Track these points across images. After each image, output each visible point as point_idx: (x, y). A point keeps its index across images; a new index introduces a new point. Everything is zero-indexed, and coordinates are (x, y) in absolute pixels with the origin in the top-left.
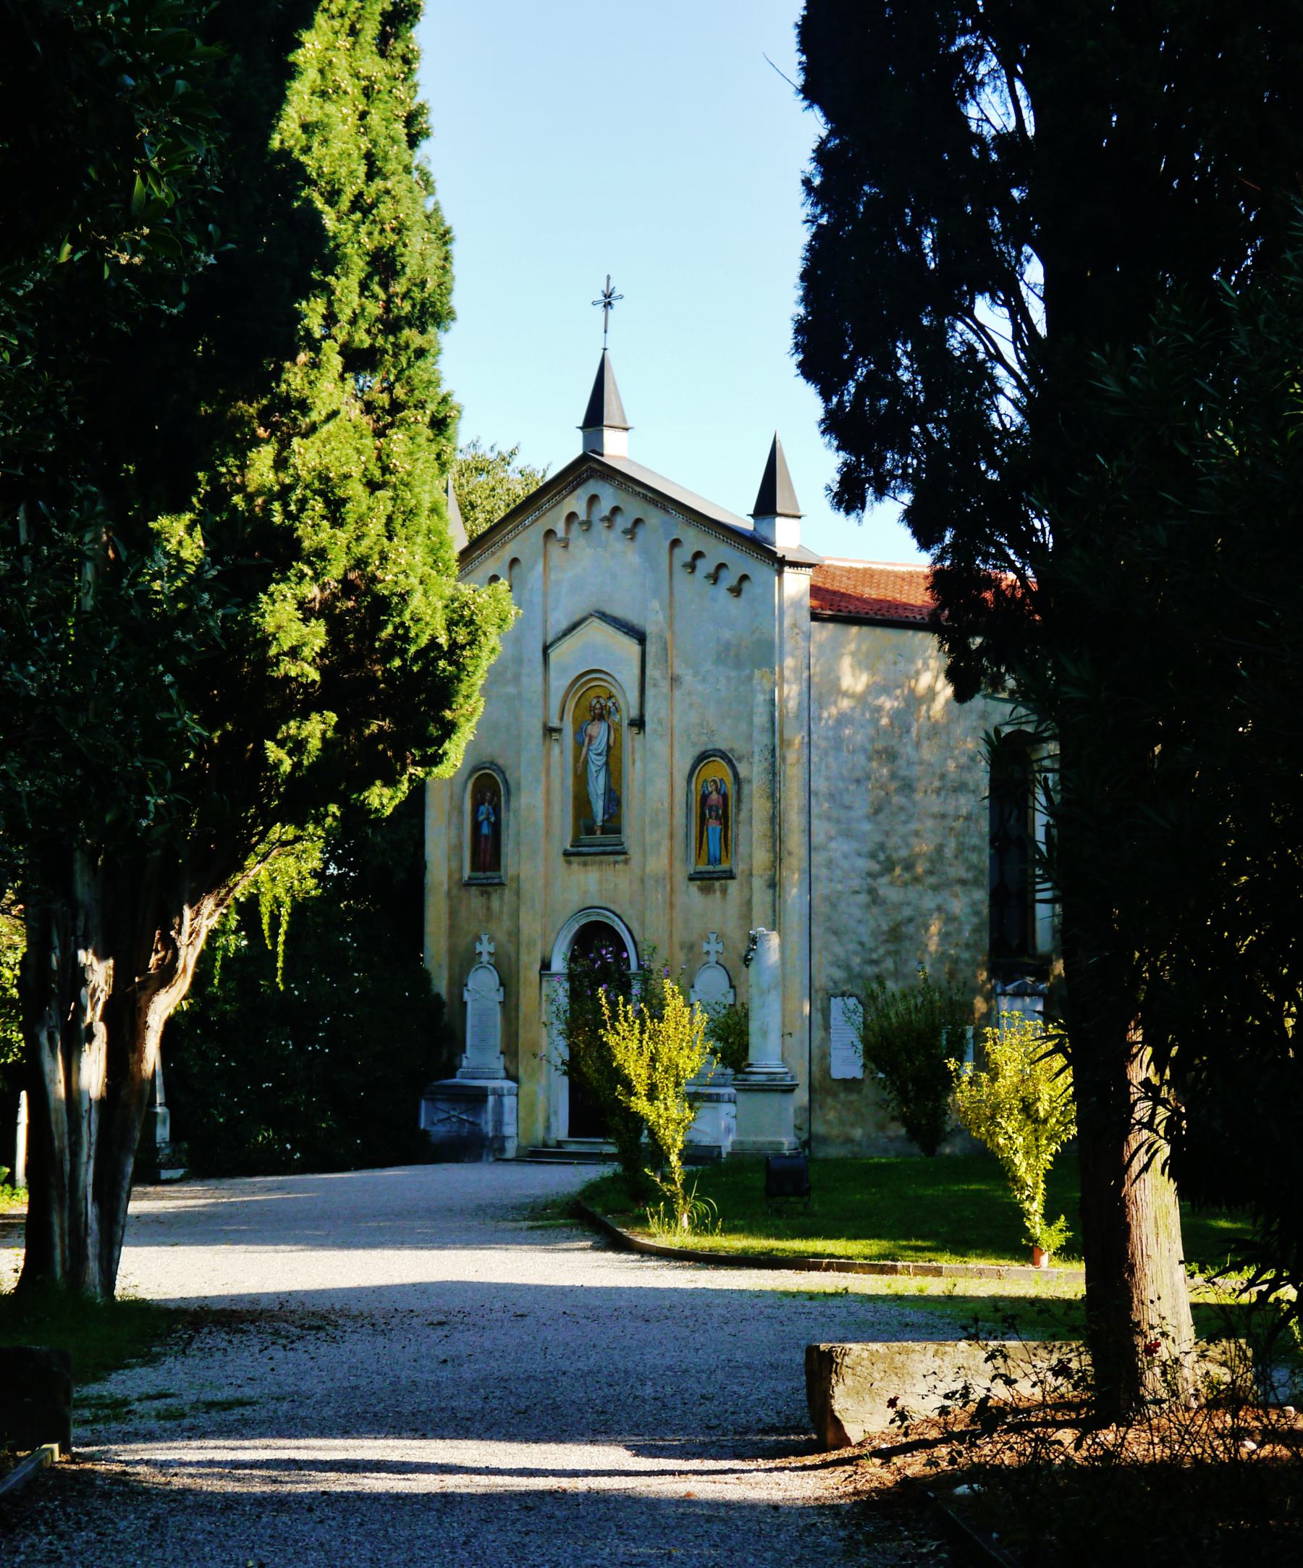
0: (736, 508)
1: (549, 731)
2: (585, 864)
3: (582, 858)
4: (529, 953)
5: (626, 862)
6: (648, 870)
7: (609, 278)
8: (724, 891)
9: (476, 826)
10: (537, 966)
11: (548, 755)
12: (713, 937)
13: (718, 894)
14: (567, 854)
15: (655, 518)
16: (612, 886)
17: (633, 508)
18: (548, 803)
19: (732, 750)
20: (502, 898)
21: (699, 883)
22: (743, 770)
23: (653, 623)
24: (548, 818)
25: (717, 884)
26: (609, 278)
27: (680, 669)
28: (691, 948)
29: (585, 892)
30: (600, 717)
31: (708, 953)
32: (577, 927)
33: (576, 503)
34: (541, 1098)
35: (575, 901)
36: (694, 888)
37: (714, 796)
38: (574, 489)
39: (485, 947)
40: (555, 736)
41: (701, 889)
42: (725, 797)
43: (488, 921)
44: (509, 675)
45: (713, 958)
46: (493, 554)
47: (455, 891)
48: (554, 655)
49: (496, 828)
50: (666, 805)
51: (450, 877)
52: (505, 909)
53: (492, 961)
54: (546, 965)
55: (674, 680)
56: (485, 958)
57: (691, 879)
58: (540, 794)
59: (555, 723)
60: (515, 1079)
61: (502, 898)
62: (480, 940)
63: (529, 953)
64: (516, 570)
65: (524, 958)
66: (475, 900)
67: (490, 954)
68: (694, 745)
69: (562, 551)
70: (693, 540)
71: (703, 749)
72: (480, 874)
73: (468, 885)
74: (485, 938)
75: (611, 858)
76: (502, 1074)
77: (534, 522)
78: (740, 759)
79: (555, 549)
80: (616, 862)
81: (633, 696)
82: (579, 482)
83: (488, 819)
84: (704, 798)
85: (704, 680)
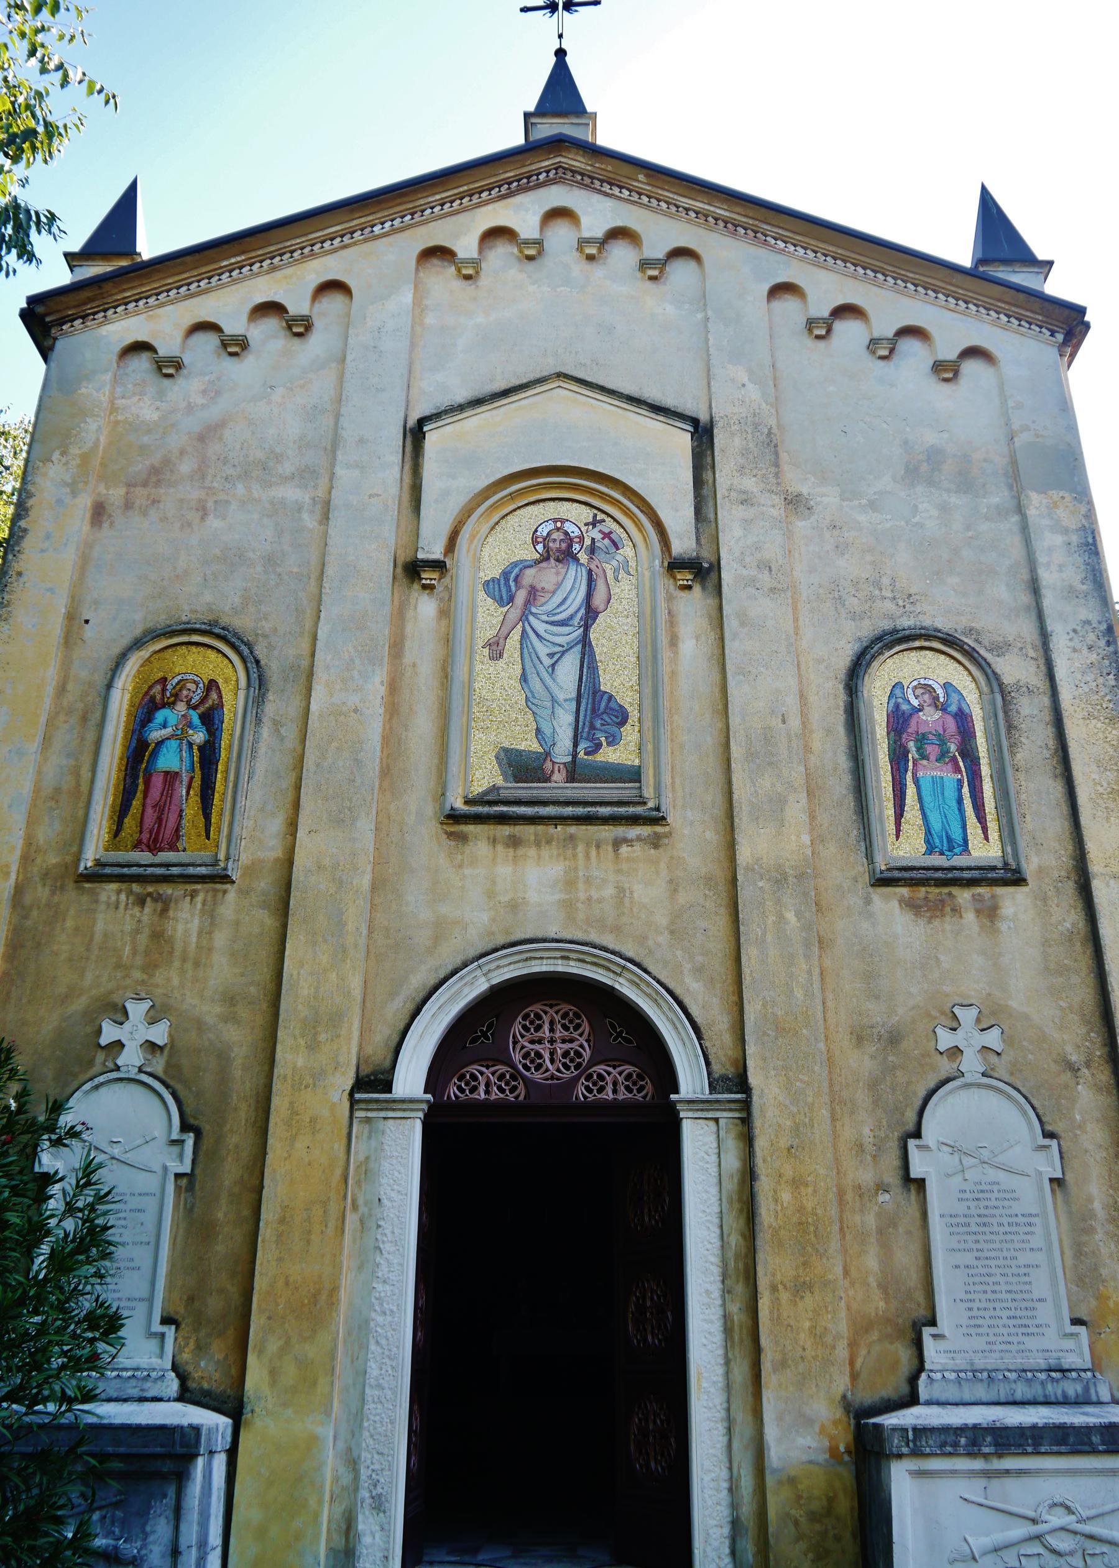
0: (959, 247)
1: (413, 570)
2: (514, 842)
3: (506, 830)
4: (313, 1046)
5: (656, 842)
6: (744, 855)
7: (524, 10)
8: (990, 913)
9: (139, 753)
10: (349, 1082)
11: (399, 616)
12: (967, 1016)
13: (970, 917)
14: (454, 817)
15: (723, 251)
16: (609, 891)
17: (661, 232)
18: (393, 708)
19: (971, 631)
20: (210, 913)
21: (904, 891)
22: (1016, 669)
23: (732, 400)
24: (392, 742)
25: (964, 896)
26: (524, 10)
27: (798, 482)
28: (894, 1039)
29: (514, 906)
30: (567, 555)
31: (955, 1052)
32: (482, 986)
33: (522, 213)
34: (330, 1461)
35: (477, 923)
36: (888, 906)
37: (930, 717)
38: (510, 194)
39: (134, 1033)
40: (427, 576)
41: (911, 905)
42: (963, 719)
43: (150, 968)
44: (287, 468)
45: (971, 1064)
46: (273, 269)
47: (42, 893)
48: (433, 438)
49: (208, 756)
50: (795, 723)
51: (26, 859)
52: (221, 938)
53: (158, 1065)
54: (374, 1082)
55: (795, 503)
56: (131, 1058)
57: (883, 881)
58: (376, 685)
59: (436, 552)
60: (234, 1407)
61: (210, 913)
62: (121, 1015)
63: (313, 1046)
64: (333, 303)
65: (290, 1056)
66: (114, 915)
67: (151, 1047)
68: (854, 616)
69: (459, 284)
70: (827, 285)
71: (887, 625)
72: (145, 857)
73: (97, 876)
74: (137, 1010)
75: (607, 832)
76: (172, 1385)
77: (394, 231)
78: (1000, 649)
79: (441, 280)
80: (617, 843)
81: (679, 519)
82: (528, 184)
83: (180, 736)
84: (899, 721)
85: (872, 505)
